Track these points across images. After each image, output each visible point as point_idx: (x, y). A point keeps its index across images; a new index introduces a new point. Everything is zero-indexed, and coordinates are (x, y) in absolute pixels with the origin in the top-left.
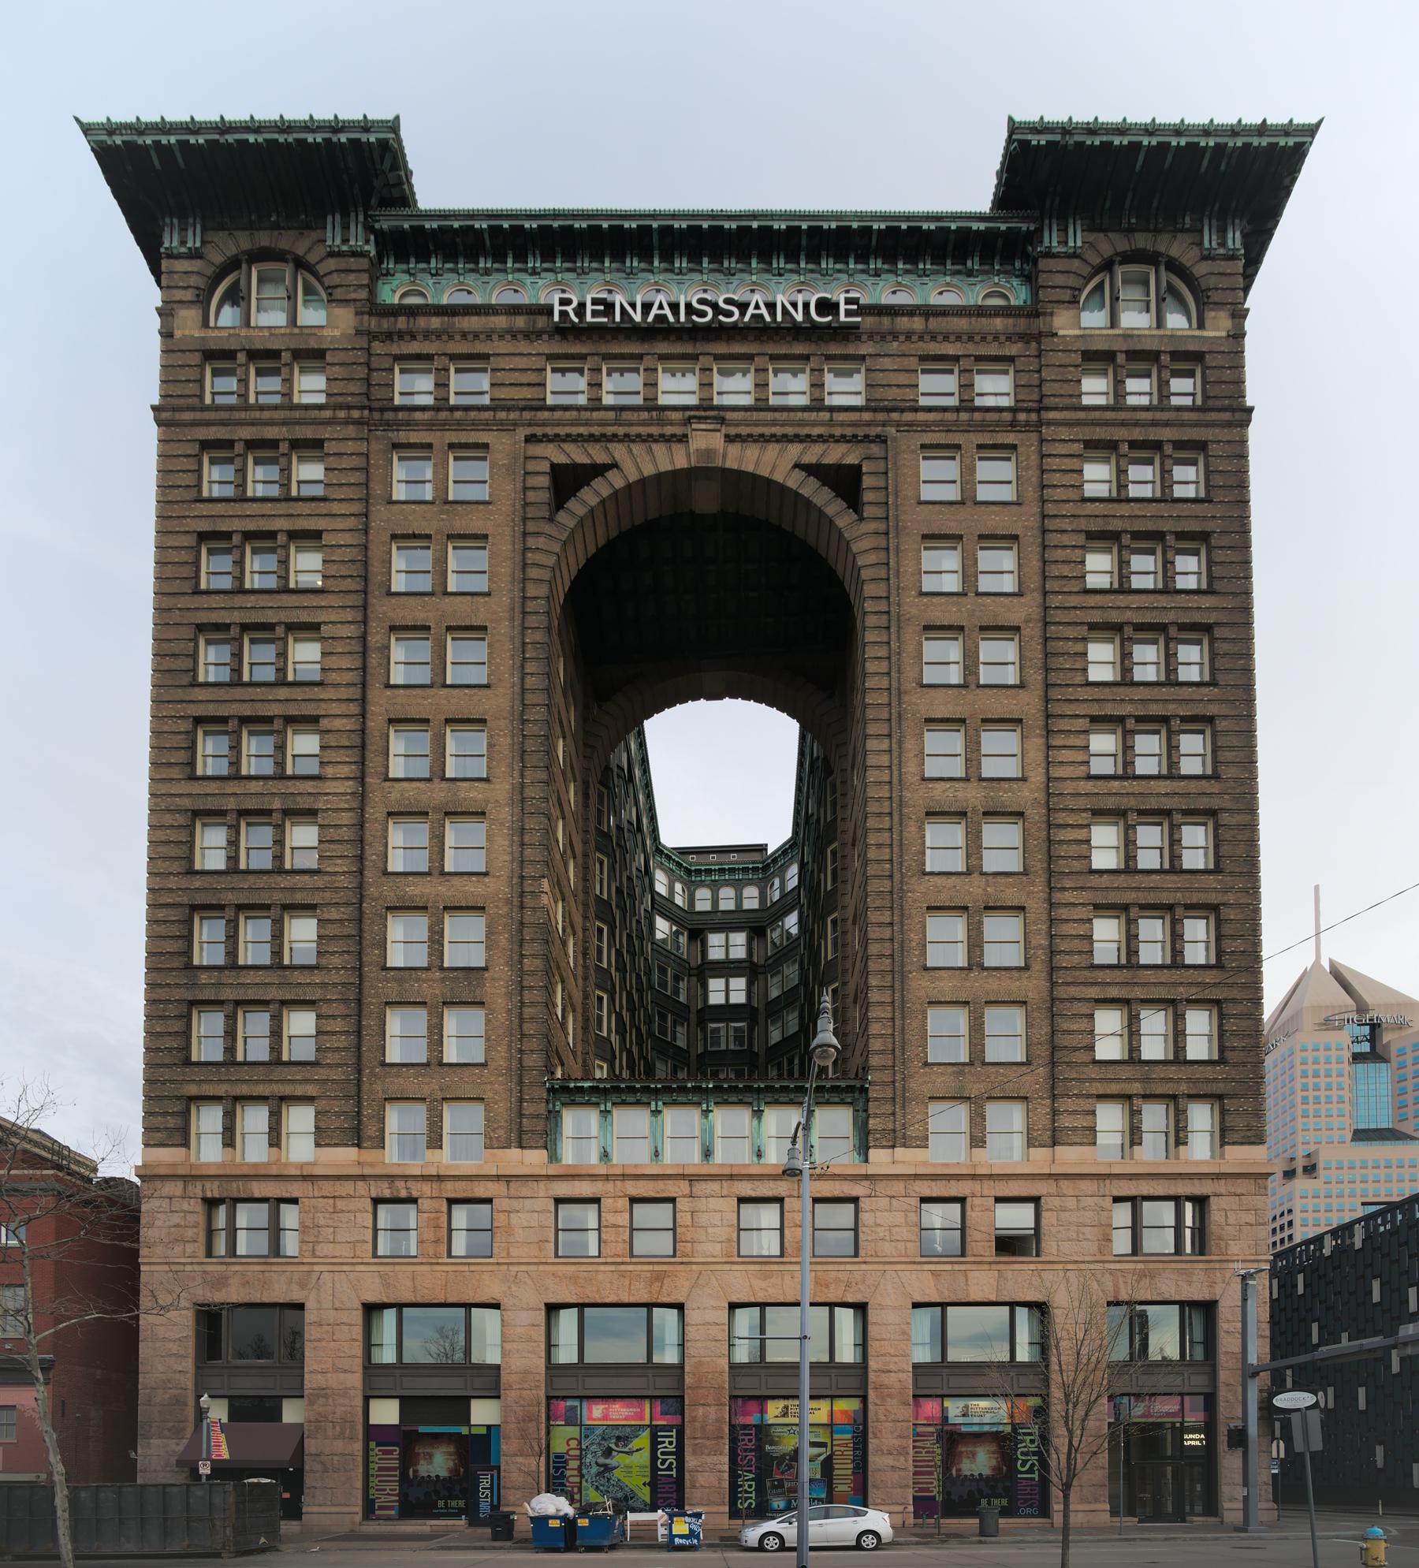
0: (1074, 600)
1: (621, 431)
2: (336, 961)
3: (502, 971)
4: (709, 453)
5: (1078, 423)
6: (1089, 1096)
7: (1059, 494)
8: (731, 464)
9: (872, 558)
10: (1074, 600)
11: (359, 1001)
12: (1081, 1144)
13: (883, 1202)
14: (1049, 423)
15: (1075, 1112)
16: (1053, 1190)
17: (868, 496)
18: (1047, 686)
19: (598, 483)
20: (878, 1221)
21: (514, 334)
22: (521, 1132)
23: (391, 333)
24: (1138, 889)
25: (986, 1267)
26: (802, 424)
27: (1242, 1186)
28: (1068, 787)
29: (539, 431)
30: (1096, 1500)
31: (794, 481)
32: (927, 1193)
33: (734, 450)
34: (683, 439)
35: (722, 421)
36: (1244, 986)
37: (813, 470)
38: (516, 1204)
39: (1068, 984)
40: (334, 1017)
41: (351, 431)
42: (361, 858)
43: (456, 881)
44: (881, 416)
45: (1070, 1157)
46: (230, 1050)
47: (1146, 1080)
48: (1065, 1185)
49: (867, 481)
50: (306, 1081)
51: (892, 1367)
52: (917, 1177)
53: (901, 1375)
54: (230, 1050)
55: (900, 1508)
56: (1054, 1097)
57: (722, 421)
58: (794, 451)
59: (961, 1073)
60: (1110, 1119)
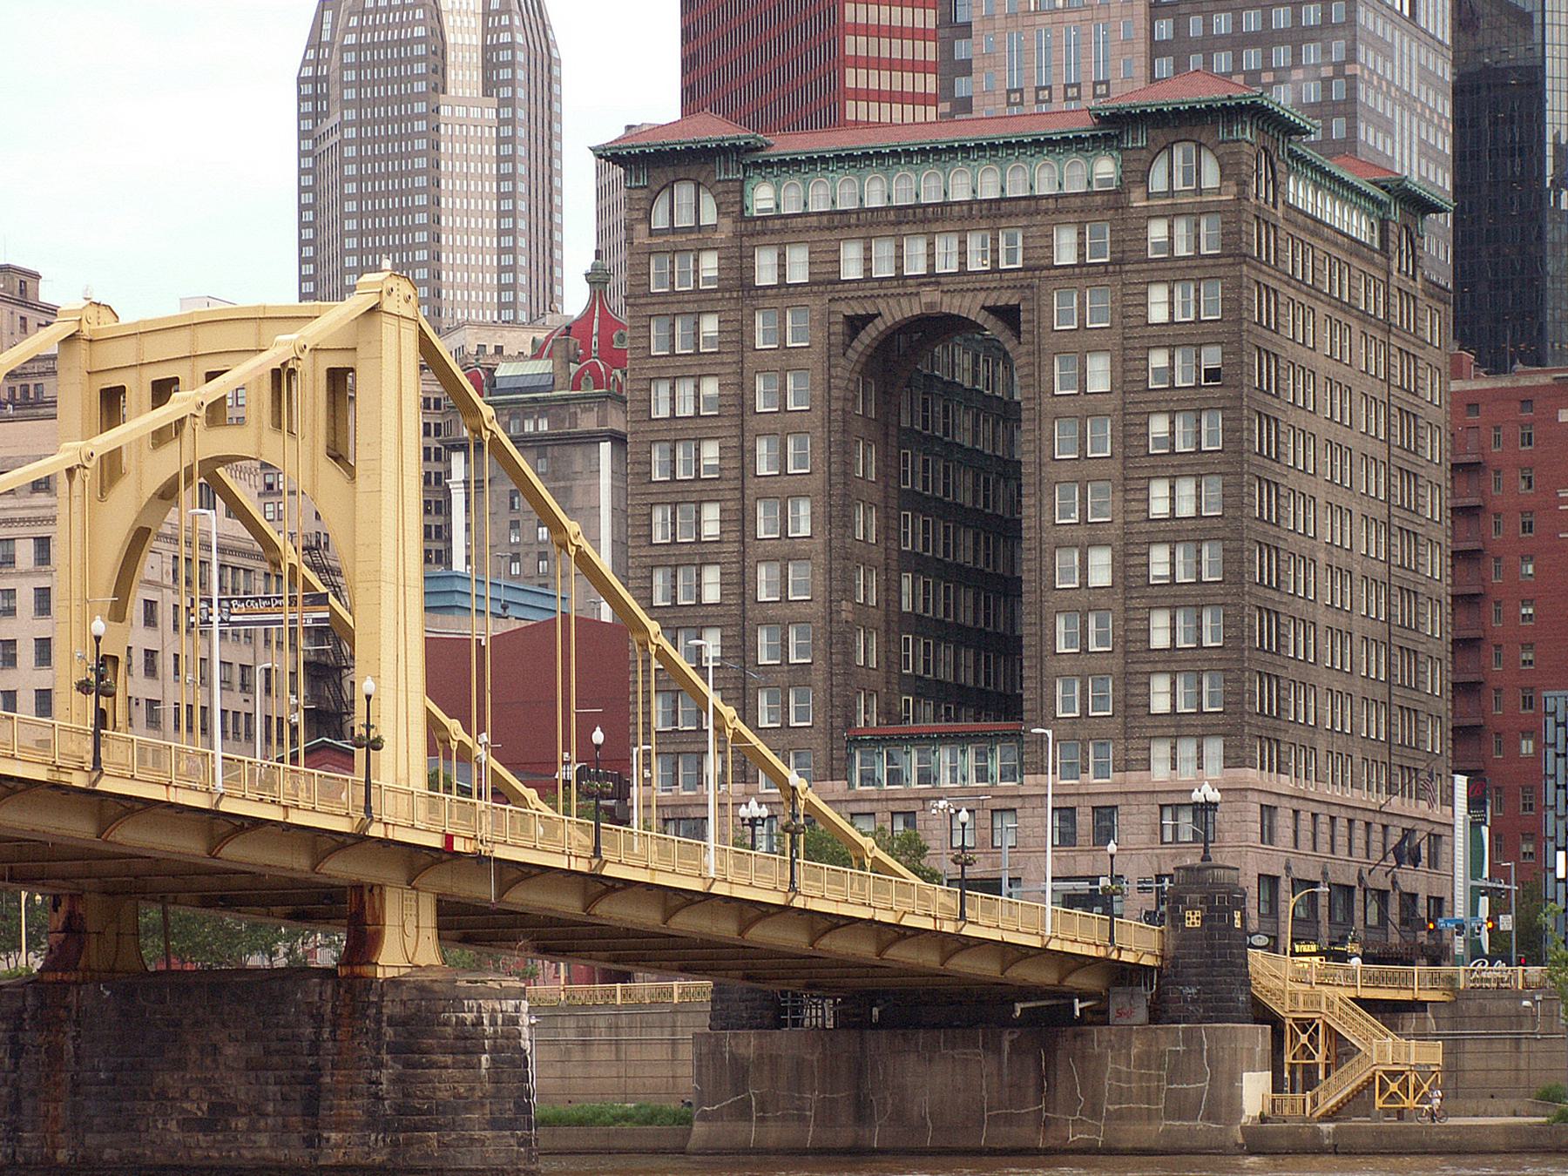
0: (1139, 397)
1: (882, 292)
3: (821, 664)
4: (931, 305)
7: (1133, 322)
8: (945, 310)
10: (1139, 397)
17: (1023, 327)
18: (1126, 458)
21: (820, 229)
23: (756, 231)
28: (1136, 528)
31: (980, 318)
33: (946, 299)
34: (918, 294)
41: (732, 304)
43: (794, 606)
44: (1029, 274)
45: (1134, 779)
47: (1178, 726)
48: (1131, 797)
57: (938, 283)
60: (1160, 751)
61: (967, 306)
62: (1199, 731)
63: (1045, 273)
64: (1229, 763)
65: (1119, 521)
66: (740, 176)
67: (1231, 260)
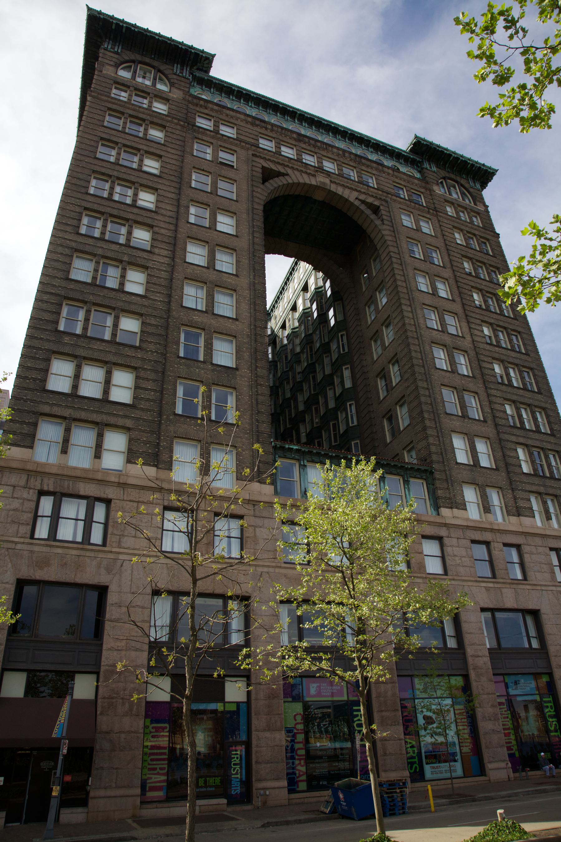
2: (152, 347)
4: (324, 183)
6: (526, 491)
11: (163, 373)
13: (454, 541)
19: (281, 178)
20: (455, 553)
25: (508, 586)
29: (258, 154)
31: (357, 203)
32: (473, 538)
35: (329, 175)
38: (259, 522)
39: (504, 433)
40: (148, 380)
42: (170, 296)
46: (75, 387)
50: (126, 417)
52: (468, 527)
54: (75, 387)
56: (513, 490)
57: (329, 175)
58: (355, 194)
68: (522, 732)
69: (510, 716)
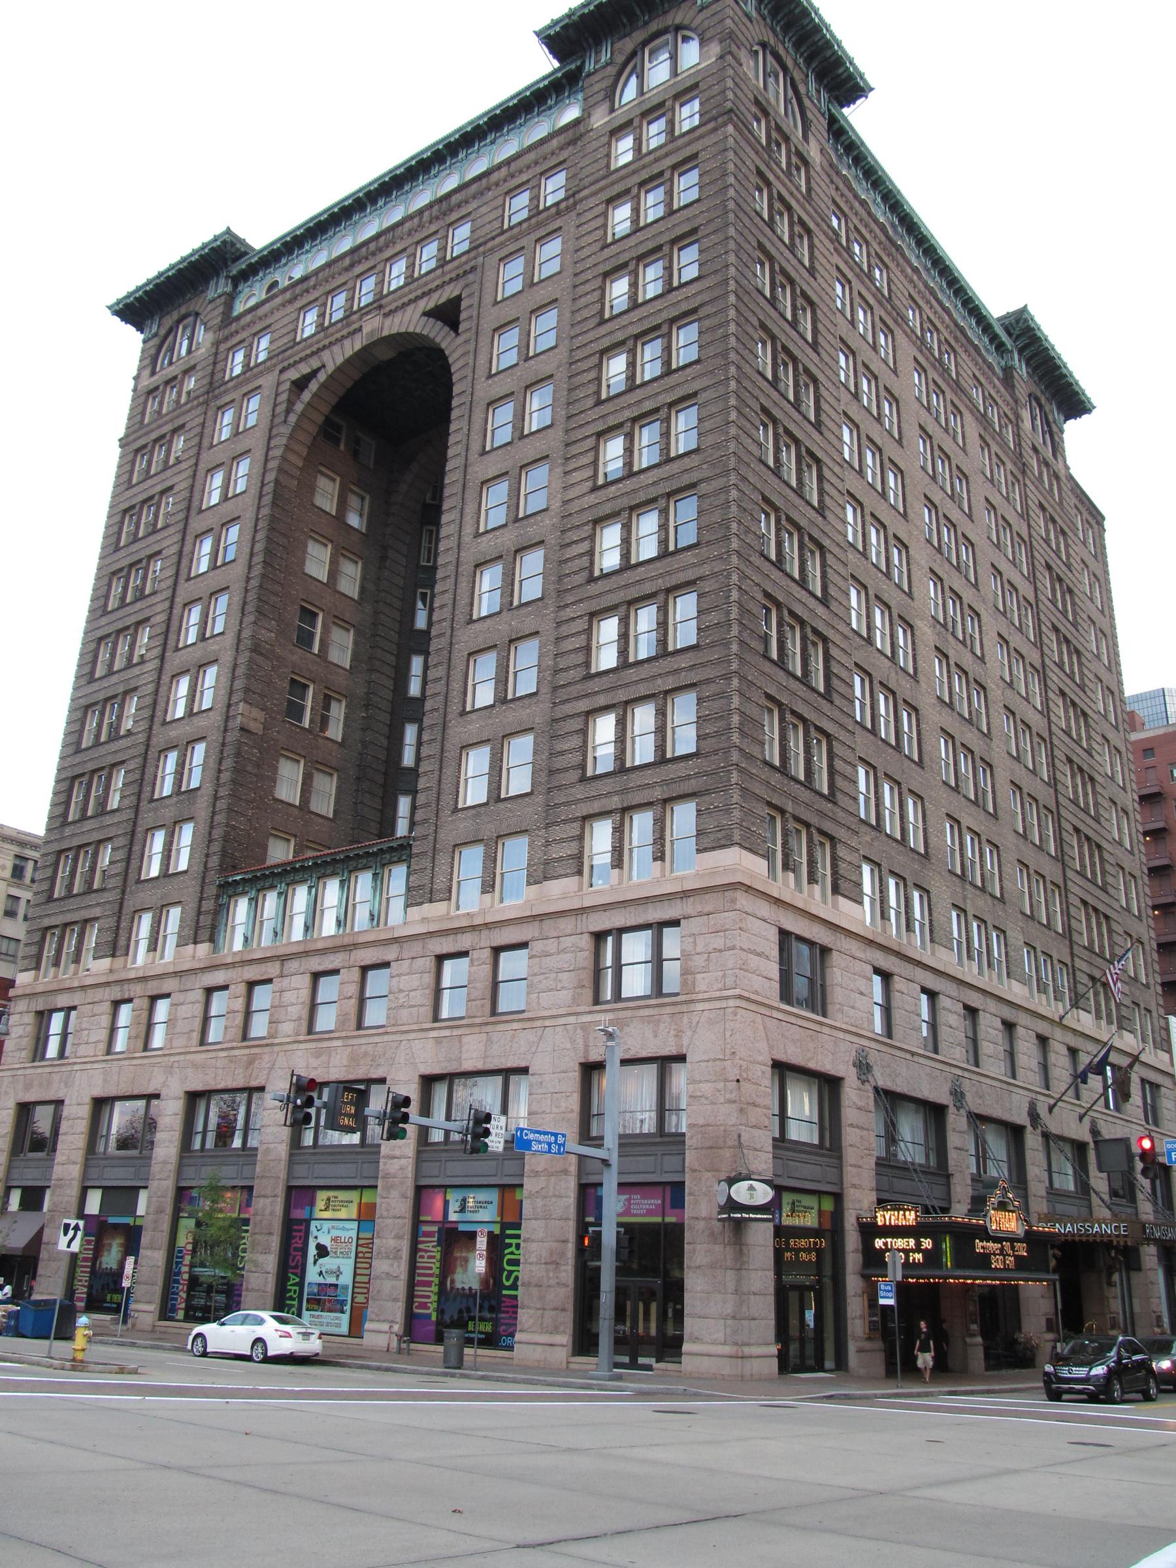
4: (372, 333)
5: (602, 189)
8: (385, 333)
9: (461, 363)
12: (566, 876)
14: (581, 200)
15: (562, 840)
16: (536, 934)
22: (197, 928)
24: (626, 586)
25: (477, 1030)
26: (426, 284)
27: (710, 902)
29: (286, 364)
30: (555, 1330)
33: (388, 321)
34: (360, 329)
36: (719, 661)
37: (427, 314)
45: (560, 891)
48: (548, 924)
49: (464, 304)
51: (397, 1153)
52: (431, 934)
53: (403, 1161)
55: (385, 1327)
59: (477, 816)
61: (410, 321)
62: (658, 794)
63: (490, 245)
64: (706, 842)
65: (556, 505)
66: (229, 289)
67: (712, 125)
68: (453, 1282)
69: (438, 1256)
